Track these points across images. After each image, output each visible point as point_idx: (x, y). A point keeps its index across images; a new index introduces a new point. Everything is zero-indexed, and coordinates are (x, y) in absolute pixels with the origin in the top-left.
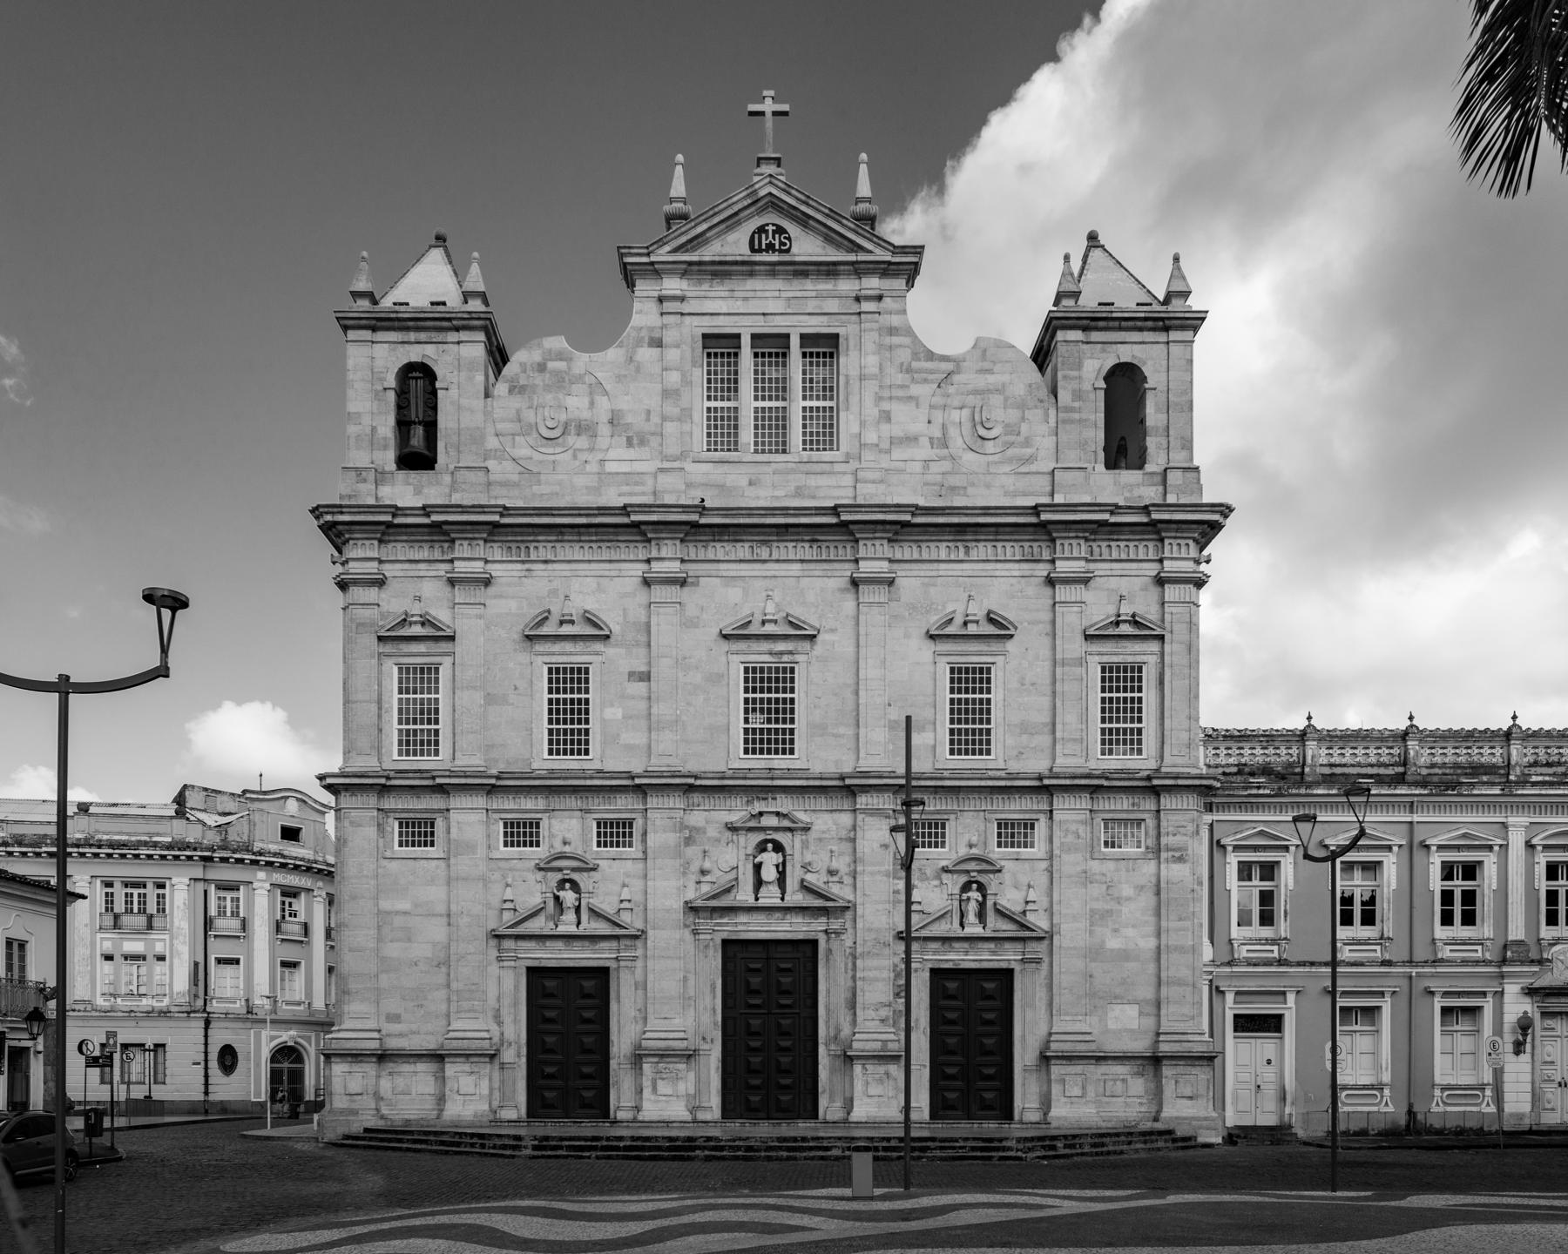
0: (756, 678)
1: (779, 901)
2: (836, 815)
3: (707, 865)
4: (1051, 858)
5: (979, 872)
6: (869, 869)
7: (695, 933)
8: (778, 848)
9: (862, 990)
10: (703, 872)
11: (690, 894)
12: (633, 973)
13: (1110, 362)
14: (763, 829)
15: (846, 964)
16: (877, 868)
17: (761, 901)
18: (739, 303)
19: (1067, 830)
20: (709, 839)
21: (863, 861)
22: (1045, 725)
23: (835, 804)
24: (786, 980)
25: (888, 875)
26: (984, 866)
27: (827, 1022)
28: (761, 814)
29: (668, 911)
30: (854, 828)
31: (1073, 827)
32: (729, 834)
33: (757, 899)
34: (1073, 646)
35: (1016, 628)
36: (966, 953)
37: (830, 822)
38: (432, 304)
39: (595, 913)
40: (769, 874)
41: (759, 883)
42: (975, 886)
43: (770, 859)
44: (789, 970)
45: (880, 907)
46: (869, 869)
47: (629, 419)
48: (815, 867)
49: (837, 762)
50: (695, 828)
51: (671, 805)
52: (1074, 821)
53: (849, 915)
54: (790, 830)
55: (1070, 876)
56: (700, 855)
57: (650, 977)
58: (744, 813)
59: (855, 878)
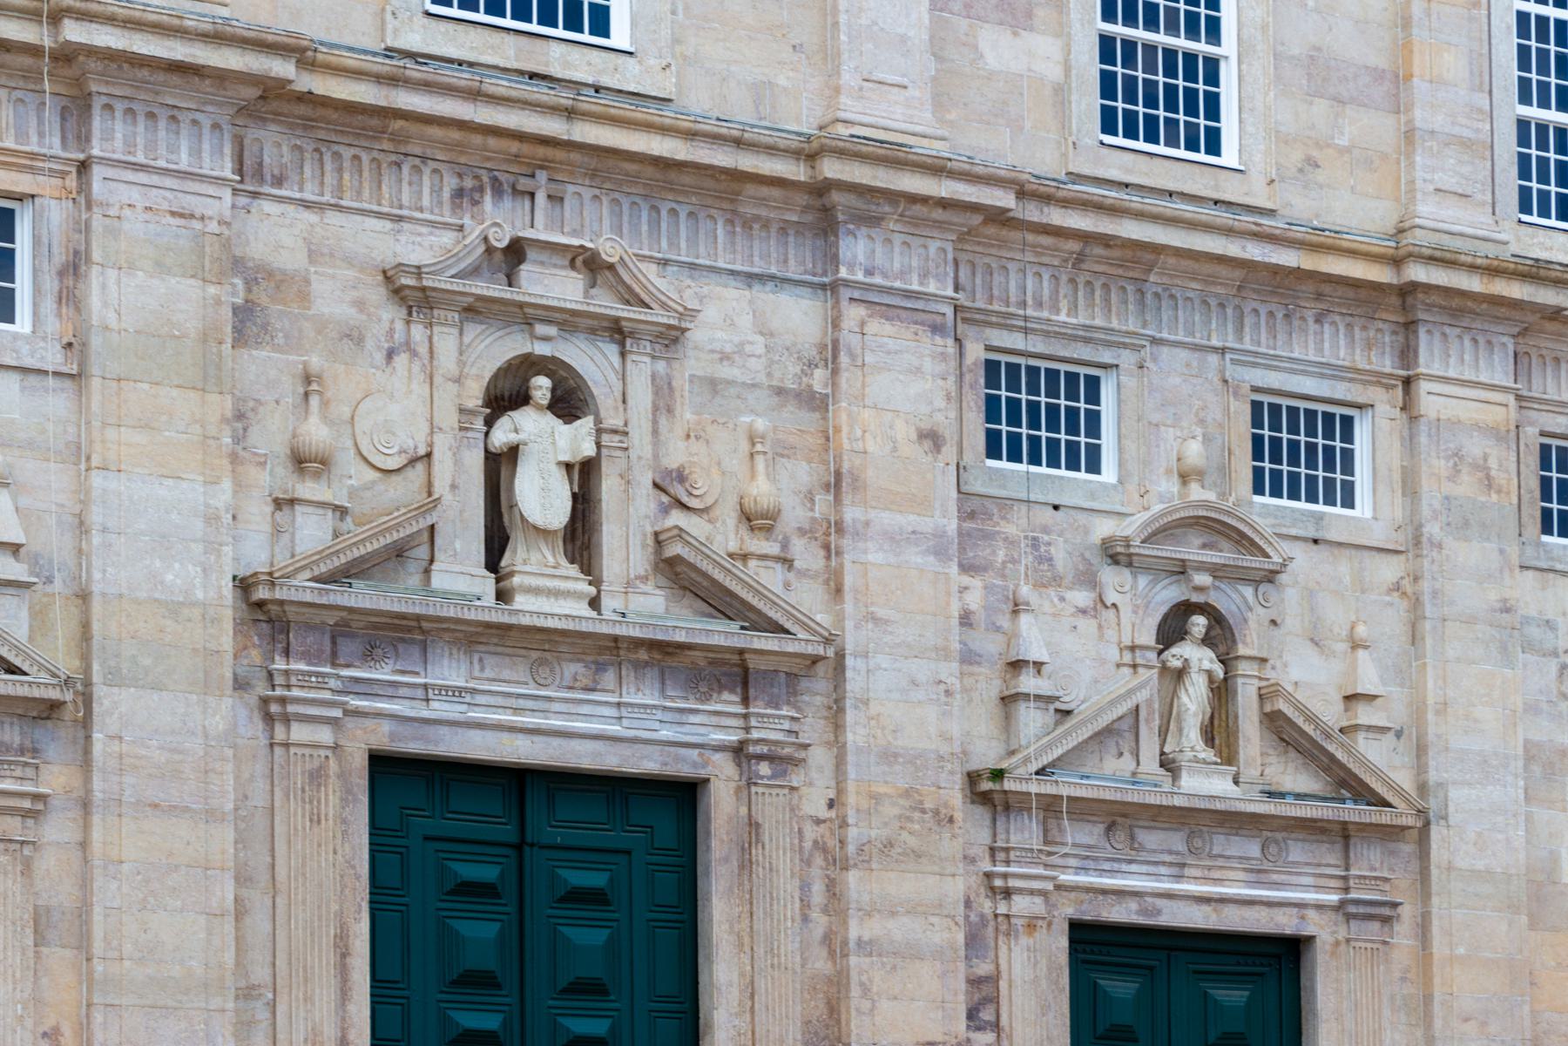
1: (584, 610)
2: (765, 296)
3: (316, 432)
4: (1414, 542)
5: (1216, 571)
6: (886, 519)
7: (273, 713)
9: (866, 990)
10: (303, 461)
12: (27, 868)
15: (805, 887)
16: (909, 521)
17: (520, 601)
19: (1457, 455)
20: (322, 325)
21: (858, 484)
22: (1378, 75)
23: (763, 255)
24: (588, 937)
25: (940, 552)
26: (1224, 555)
28: (516, 252)
29: (174, 609)
30: (830, 354)
31: (1475, 447)
32: (389, 314)
33: (502, 596)
36: (1179, 870)
37: (745, 321)
42: (1199, 623)
44: (595, 898)
45: (923, 670)
46: (886, 519)
48: (705, 485)
49: (761, 91)
50: (270, 274)
51: (184, 161)
52: (1476, 426)
53: (816, 693)
54: (617, 332)
55: (1470, 621)
56: (290, 389)
57: (107, 893)
58: (447, 238)
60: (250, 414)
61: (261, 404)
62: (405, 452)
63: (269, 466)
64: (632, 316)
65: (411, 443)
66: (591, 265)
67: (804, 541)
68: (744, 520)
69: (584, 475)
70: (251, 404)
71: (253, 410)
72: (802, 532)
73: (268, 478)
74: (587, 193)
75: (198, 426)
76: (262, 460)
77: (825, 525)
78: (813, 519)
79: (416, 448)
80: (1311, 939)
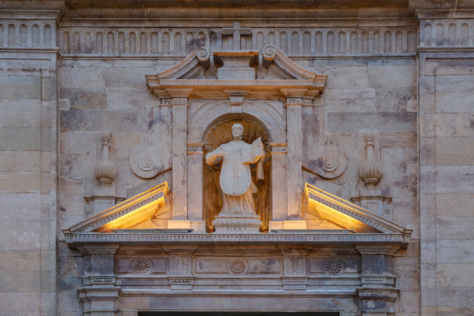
59: (415, 192)
60: (73, 161)
61: (78, 155)
62: (157, 168)
63: (83, 184)
64: (284, 84)
65: (160, 164)
67: (399, 188)
68: (361, 181)
70: (74, 156)
71: (74, 159)
72: (398, 184)
73: (83, 190)
74: (266, 32)
75: (37, 167)
76: (80, 181)
77: (413, 179)
78: (406, 177)
79: (163, 166)
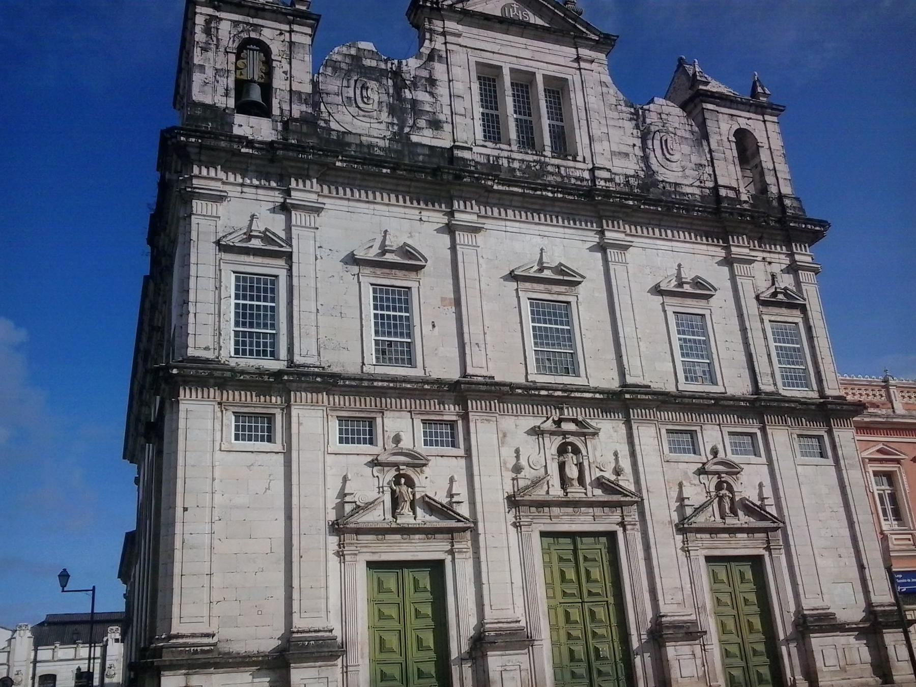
0: (540, 310)
8: (576, 451)
11: (509, 489)
13: (736, 127)
14: (565, 434)
17: (569, 495)
18: (499, 47)
27: (635, 607)
34: (751, 307)
35: (716, 290)
38: (267, 2)
39: (431, 506)
40: (572, 472)
41: (564, 482)
43: (571, 459)
47: (427, 108)
54: (584, 434)
66: (575, 421)
69: (580, 466)
80: (763, 555)
